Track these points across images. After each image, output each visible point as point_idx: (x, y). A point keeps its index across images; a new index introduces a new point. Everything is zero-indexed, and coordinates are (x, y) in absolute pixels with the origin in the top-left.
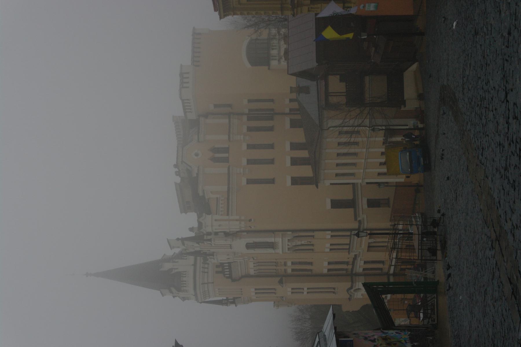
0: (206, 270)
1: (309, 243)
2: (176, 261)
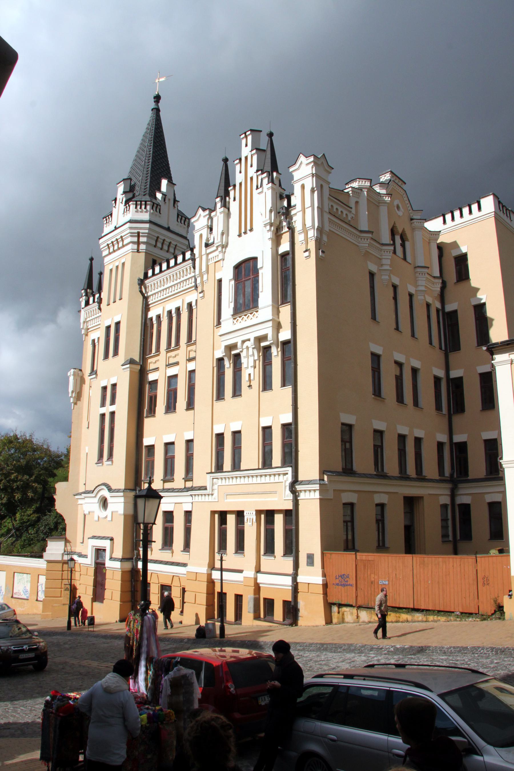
0: (159, 245)
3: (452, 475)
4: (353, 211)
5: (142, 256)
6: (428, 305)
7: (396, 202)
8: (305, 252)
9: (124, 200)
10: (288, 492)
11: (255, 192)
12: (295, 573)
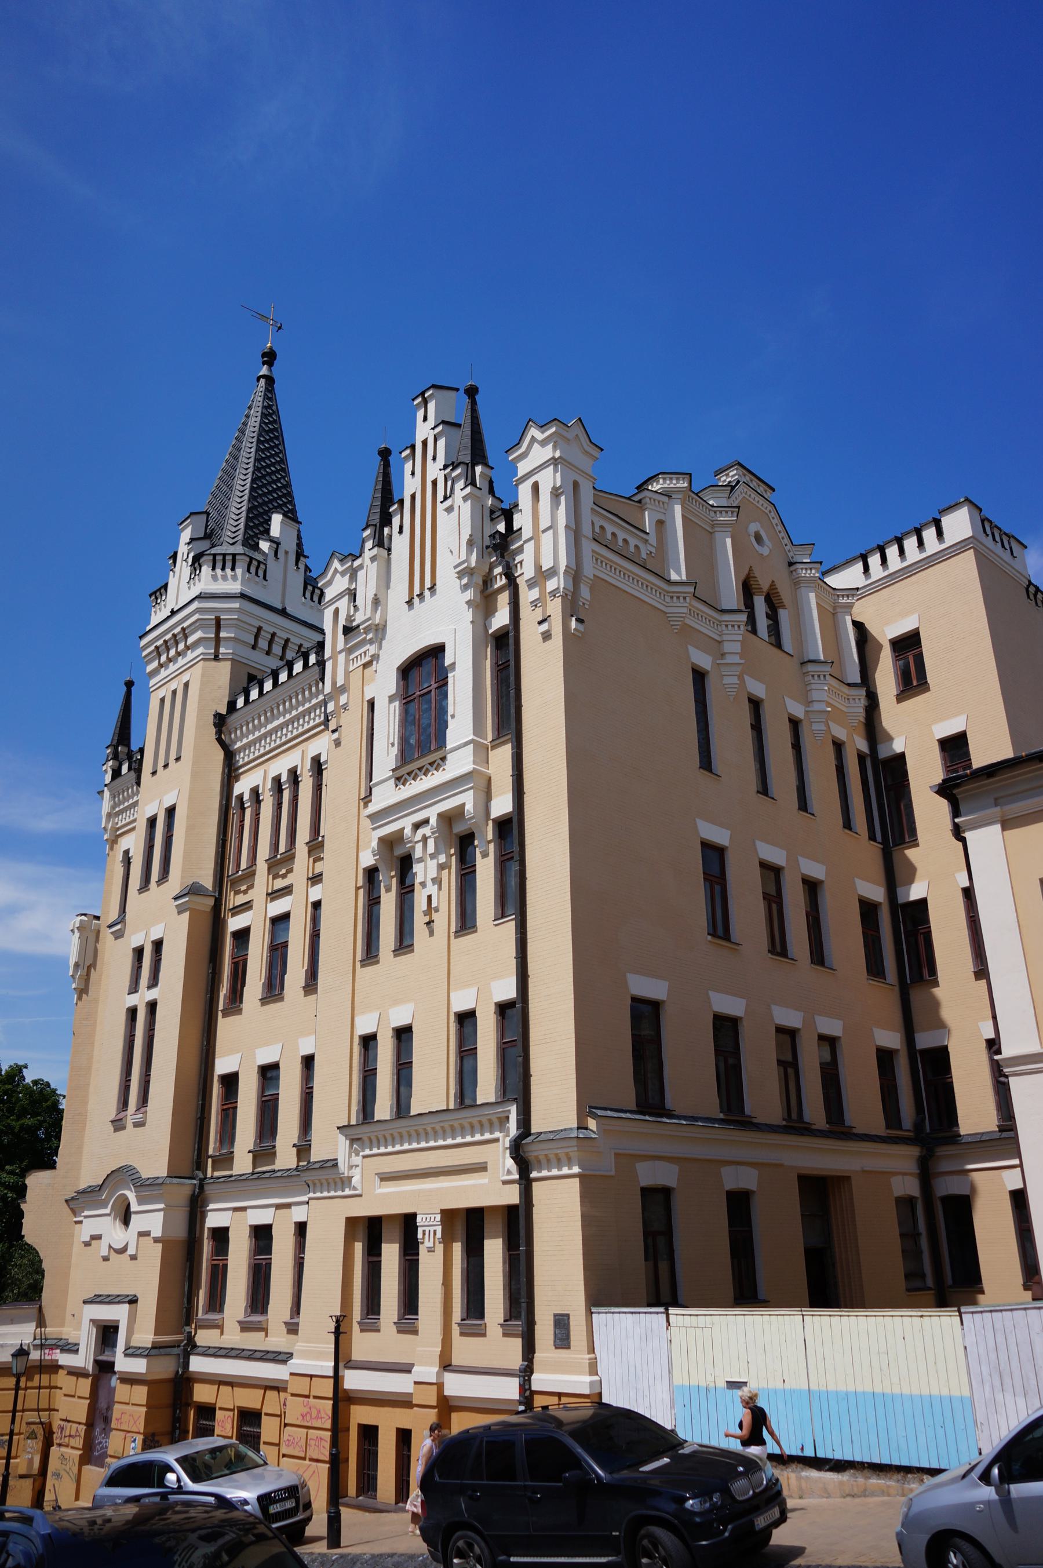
0: (263, 644)
1: (419, 920)
2: (302, 566)
3: (918, 1126)
4: (652, 539)
5: (225, 667)
6: (838, 746)
7: (754, 527)
8: (540, 623)
9: (191, 555)
10: (510, 1163)
11: (441, 507)
12: (527, 1366)
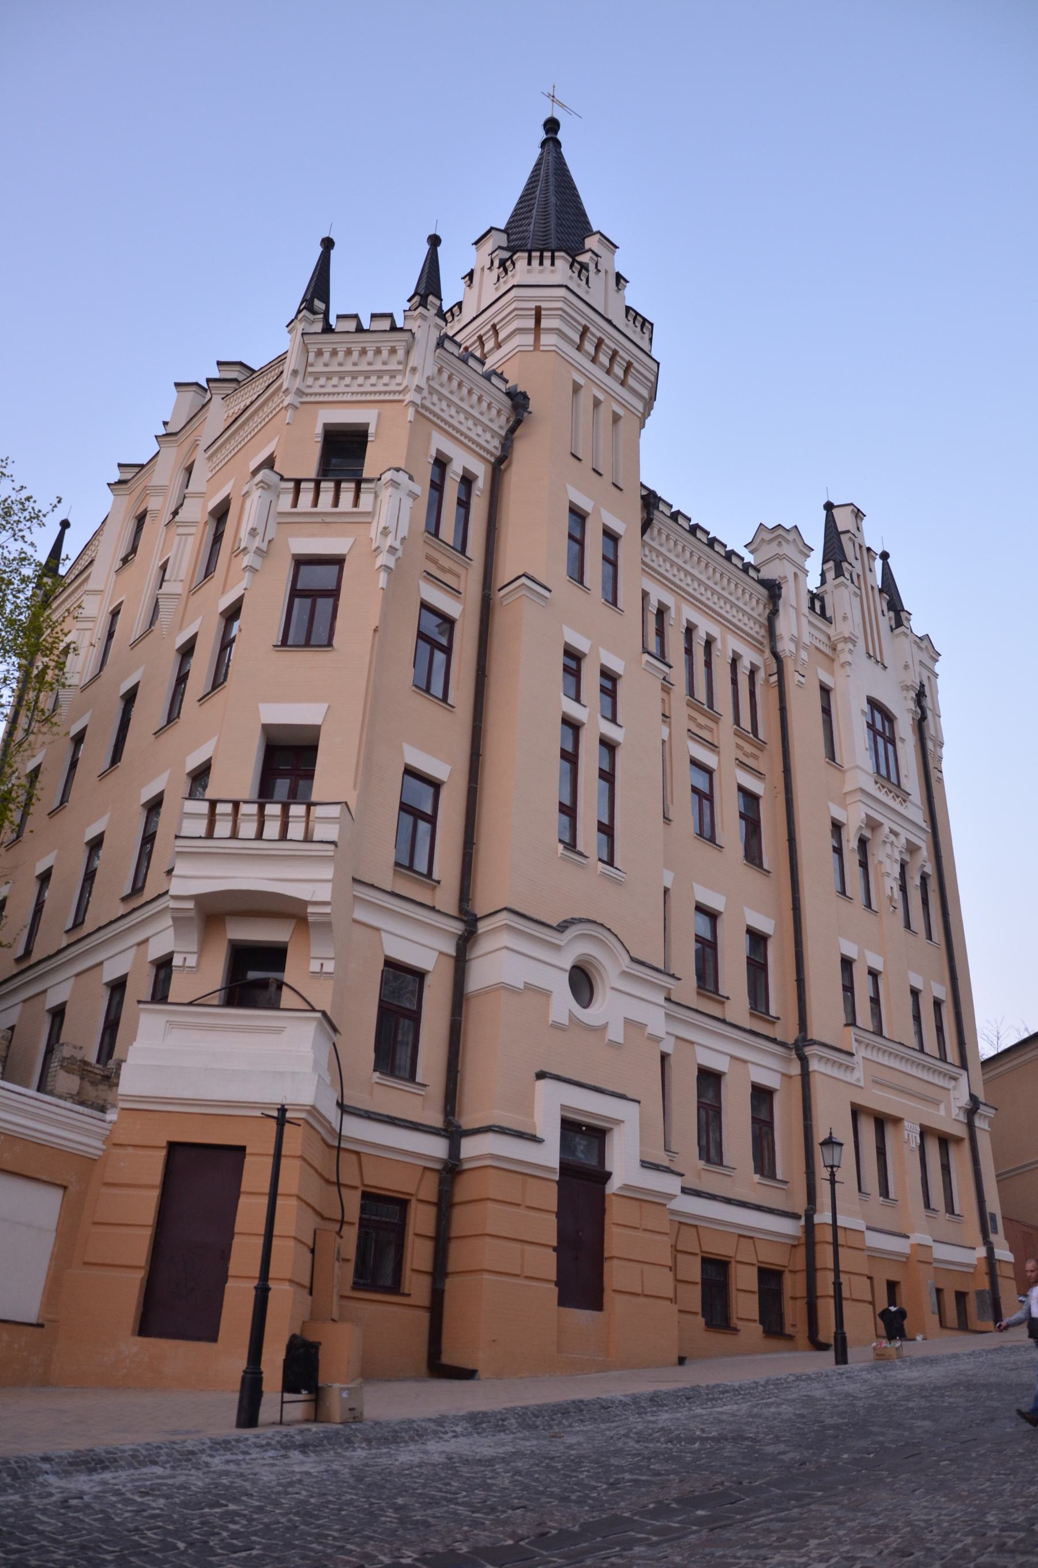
0: (589, 347)
9: (496, 263)
